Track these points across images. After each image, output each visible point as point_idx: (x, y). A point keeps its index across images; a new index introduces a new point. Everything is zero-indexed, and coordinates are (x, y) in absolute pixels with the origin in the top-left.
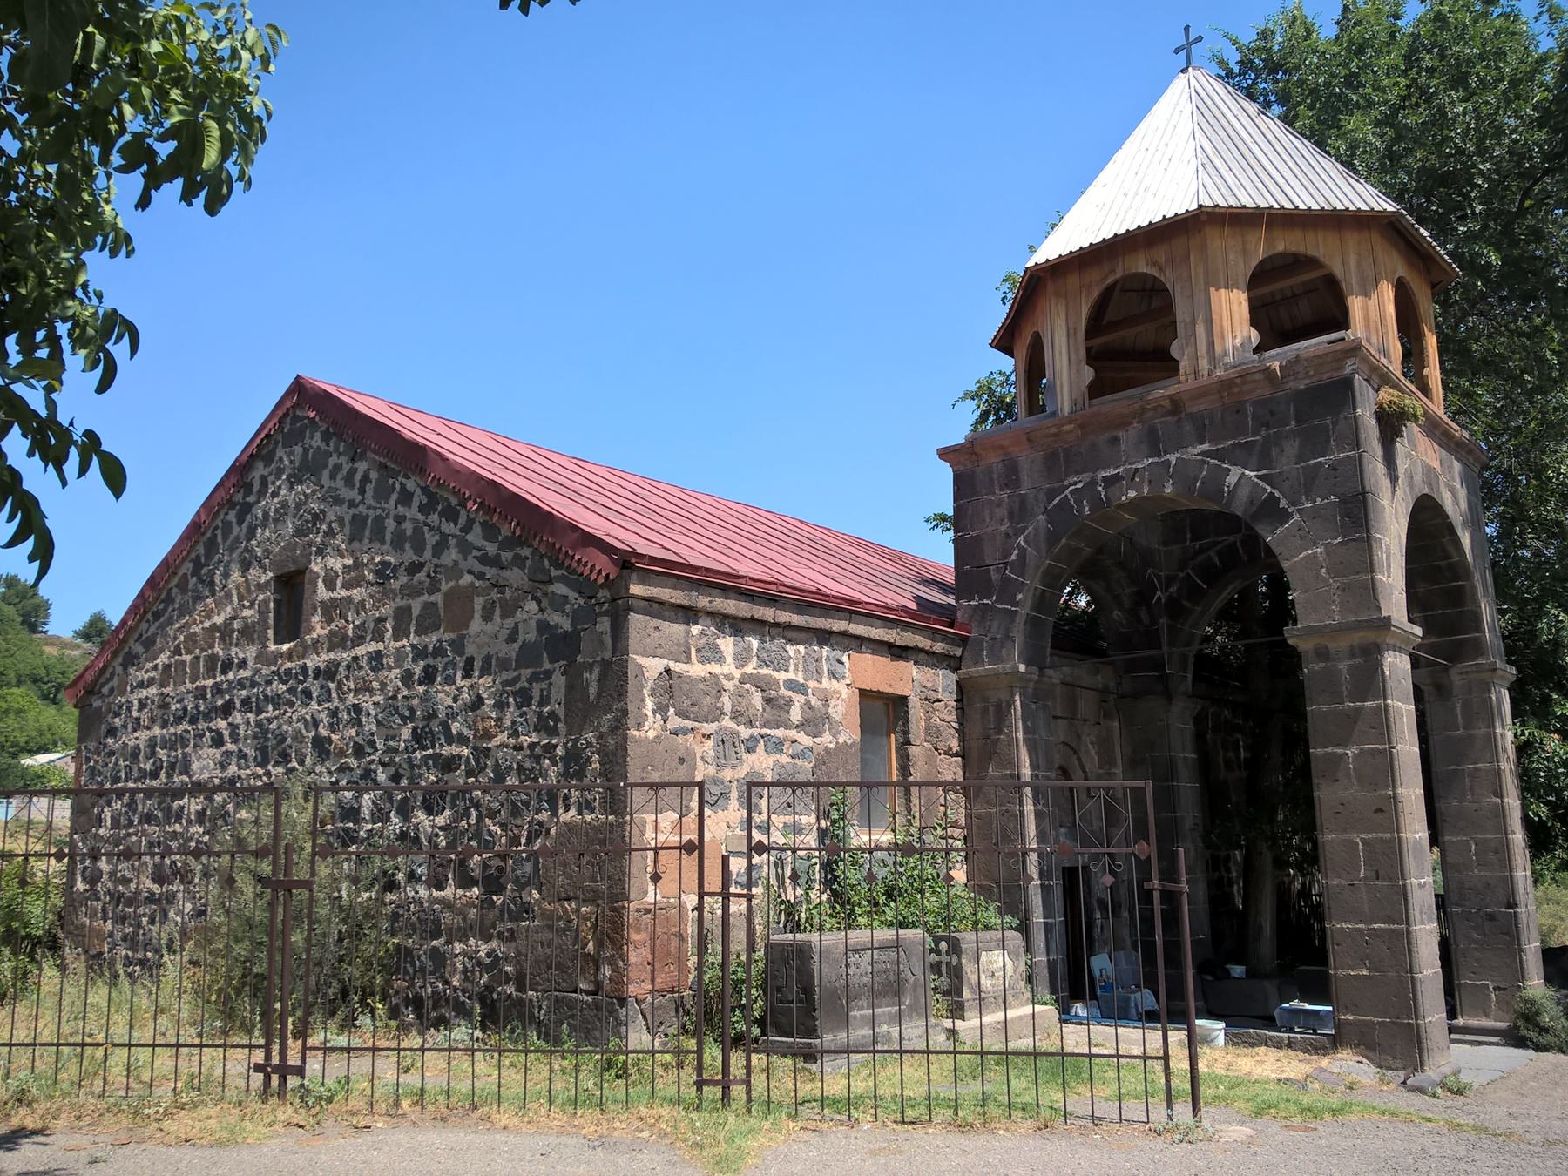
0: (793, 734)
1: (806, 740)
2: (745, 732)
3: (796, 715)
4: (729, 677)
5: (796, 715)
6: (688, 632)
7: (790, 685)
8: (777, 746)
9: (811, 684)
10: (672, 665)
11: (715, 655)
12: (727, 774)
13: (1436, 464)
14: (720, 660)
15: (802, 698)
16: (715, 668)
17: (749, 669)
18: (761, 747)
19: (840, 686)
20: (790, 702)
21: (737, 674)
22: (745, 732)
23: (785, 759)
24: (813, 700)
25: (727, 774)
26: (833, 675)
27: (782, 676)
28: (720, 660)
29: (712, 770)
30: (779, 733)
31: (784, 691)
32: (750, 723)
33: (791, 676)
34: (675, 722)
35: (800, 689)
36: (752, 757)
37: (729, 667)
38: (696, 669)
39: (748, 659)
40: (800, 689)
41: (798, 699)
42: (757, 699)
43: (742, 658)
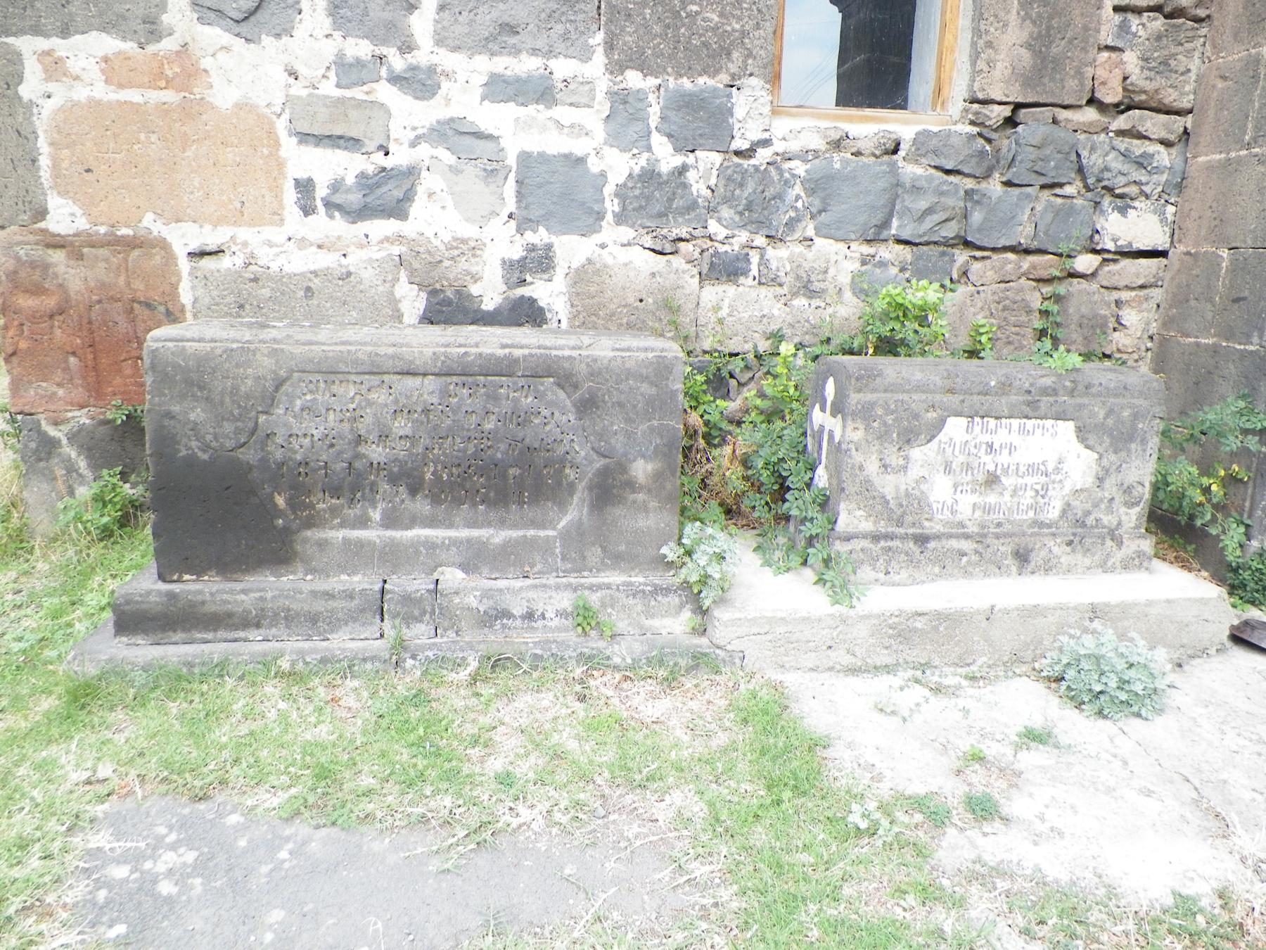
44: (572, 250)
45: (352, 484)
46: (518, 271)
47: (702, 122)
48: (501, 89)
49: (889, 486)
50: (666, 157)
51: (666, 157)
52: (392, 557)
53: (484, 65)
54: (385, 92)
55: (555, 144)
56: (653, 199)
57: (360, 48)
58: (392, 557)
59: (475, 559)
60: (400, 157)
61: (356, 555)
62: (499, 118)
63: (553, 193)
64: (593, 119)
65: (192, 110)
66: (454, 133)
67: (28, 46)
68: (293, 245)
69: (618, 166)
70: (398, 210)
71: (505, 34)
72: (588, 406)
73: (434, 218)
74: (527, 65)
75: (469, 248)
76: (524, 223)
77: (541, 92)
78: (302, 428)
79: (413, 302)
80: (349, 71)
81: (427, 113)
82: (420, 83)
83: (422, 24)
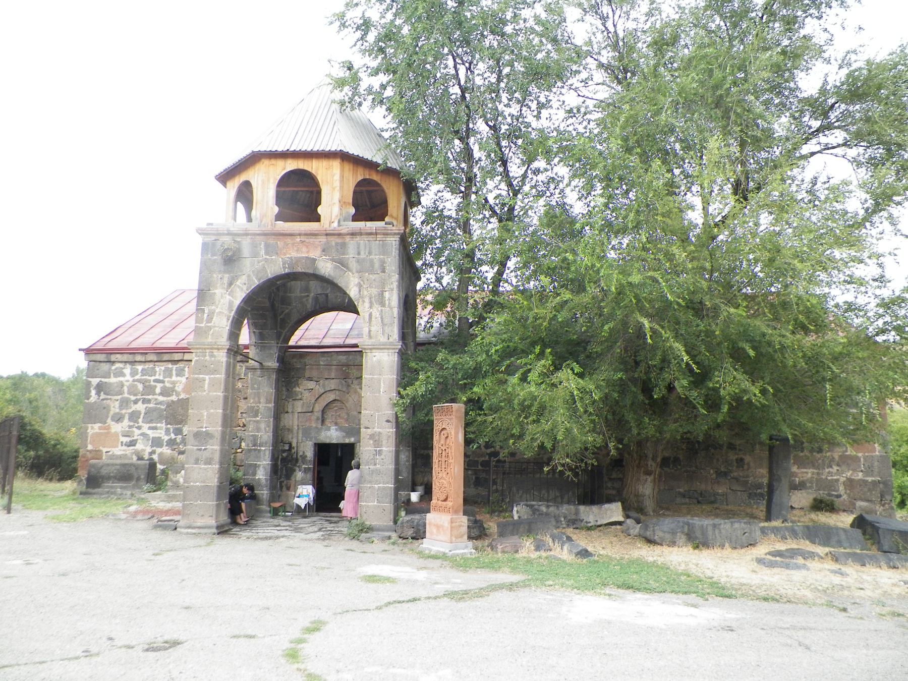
0: (156, 397)
1: (161, 398)
2: (133, 398)
3: (158, 390)
4: (128, 381)
5: (158, 390)
6: (110, 369)
7: (155, 381)
8: (149, 401)
9: (166, 380)
10: (103, 380)
11: (120, 373)
12: (123, 412)
13: (315, 254)
14: (124, 375)
15: (162, 385)
16: (121, 379)
17: (137, 377)
18: (140, 403)
19: (183, 380)
20: (156, 387)
21: (131, 379)
22: (133, 398)
23: (151, 405)
24: (168, 385)
25: (123, 412)
26: (177, 375)
27: (153, 378)
28: (124, 375)
29: (117, 410)
30: (150, 397)
31: (152, 383)
32: (135, 395)
33: (157, 377)
34: (103, 396)
35: (163, 382)
36: (136, 406)
37: (128, 377)
38: (113, 380)
39: (137, 374)
40: (163, 382)
41: (159, 385)
42: (140, 387)
43: (134, 373)
44: (159, 450)
45: (108, 478)
46: (151, 453)
47: (178, 432)
48: (150, 428)
49: (174, 479)
50: (173, 436)
51: (173, 436)
52: (112, 487)
53: (148, 425)
54: (135, 429)
55: (157, 435)
56: (171, 443)
57: (132, 424)
58: (112, 487)
59: (121, 488)
60: (135, 438)
61: (108, 487)
62: (150, 432)
63: (157, 442)
64: (163, 432)
65: (108, 433)
66: (143, 434)
67: (90, 425)
68: (119, 451)
69: (166, 438)
70: (134, 445)
71: (151, 421)
72: (136, 469)
73: (139, 446)
74: (154, 425)
75: (144, 450)
76: (152, 447)
77: (155, 428)
78: (104, 472)
79: (135, 458)
80: (130, 427)
81: (140, 432)
82: (139, 428)
83: (140, 420)
